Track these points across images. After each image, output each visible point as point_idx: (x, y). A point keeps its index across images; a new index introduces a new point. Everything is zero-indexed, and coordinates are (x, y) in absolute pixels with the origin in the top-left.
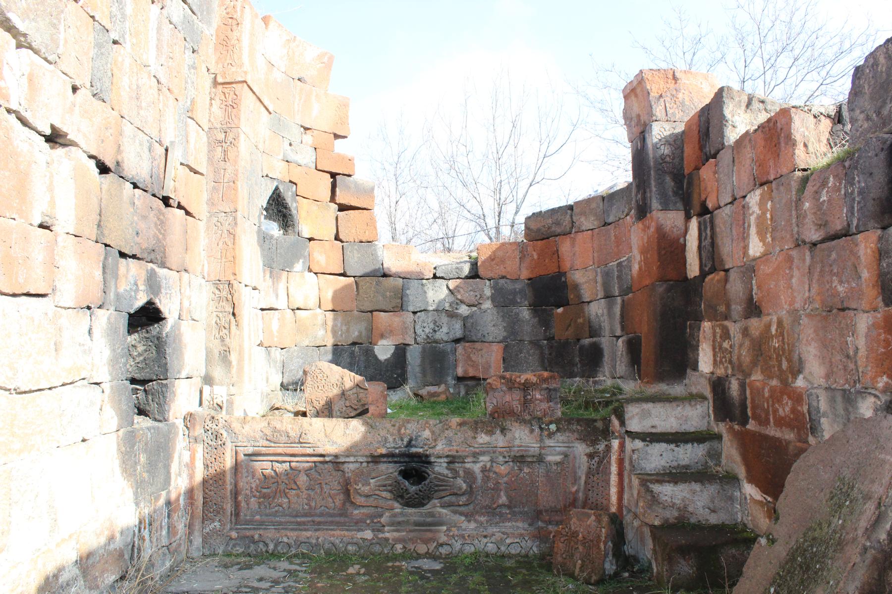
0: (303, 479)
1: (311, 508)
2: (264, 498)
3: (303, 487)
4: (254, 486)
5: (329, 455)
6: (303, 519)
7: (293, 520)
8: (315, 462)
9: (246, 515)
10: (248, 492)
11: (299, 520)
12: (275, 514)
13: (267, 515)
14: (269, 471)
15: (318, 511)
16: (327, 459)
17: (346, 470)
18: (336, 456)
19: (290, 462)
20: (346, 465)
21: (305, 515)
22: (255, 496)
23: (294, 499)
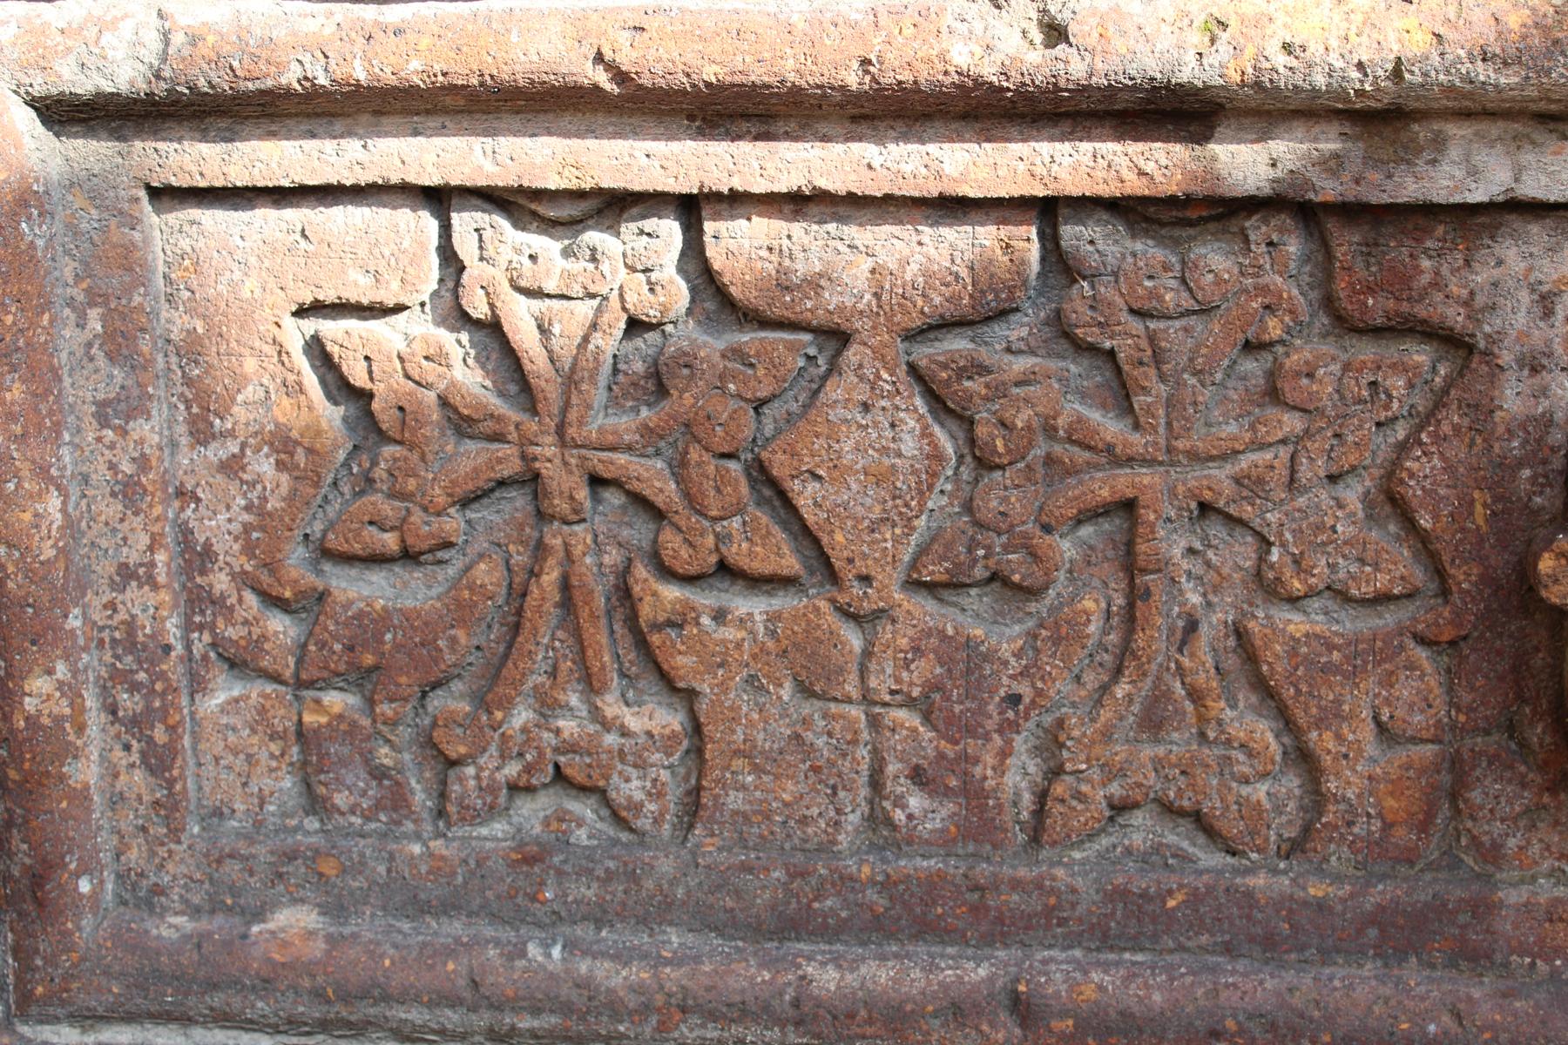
0: (871, 451)
1: (979, 820)
2: (364, 678)
3: (880, 555)
4: (220, 524)
5: (1264, 107)
6: (880, 973)
7: (750, 974)
8: (1047, 211)
9: (145, 897)
10: (155, 610)
11: (827, 979)
12: (520, 888)
13: (412, 900)
14: (409, 349)
15: (1074, 870)
16: (1244, 162)
17: (1516, 319)
18: (1386, 115)
19: (691, 208)
20: (1516, 257)
21: (912, 917)
22: (239, 663)
23: (760, 715)
